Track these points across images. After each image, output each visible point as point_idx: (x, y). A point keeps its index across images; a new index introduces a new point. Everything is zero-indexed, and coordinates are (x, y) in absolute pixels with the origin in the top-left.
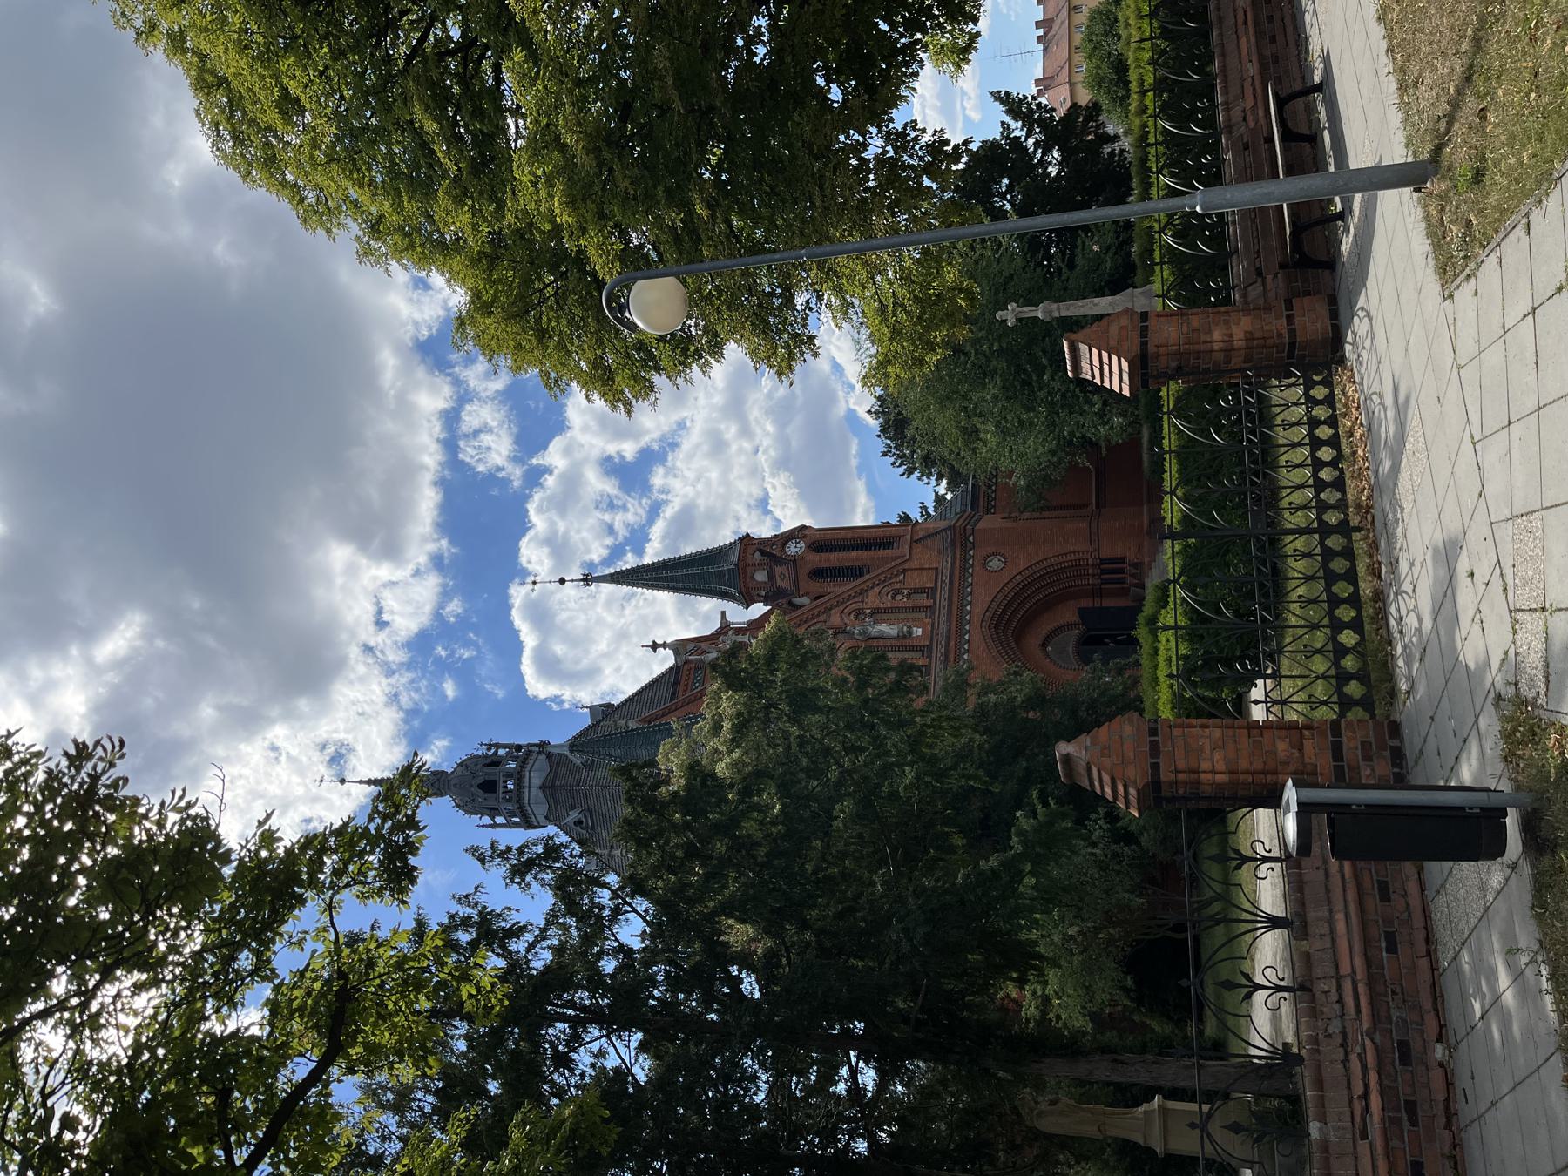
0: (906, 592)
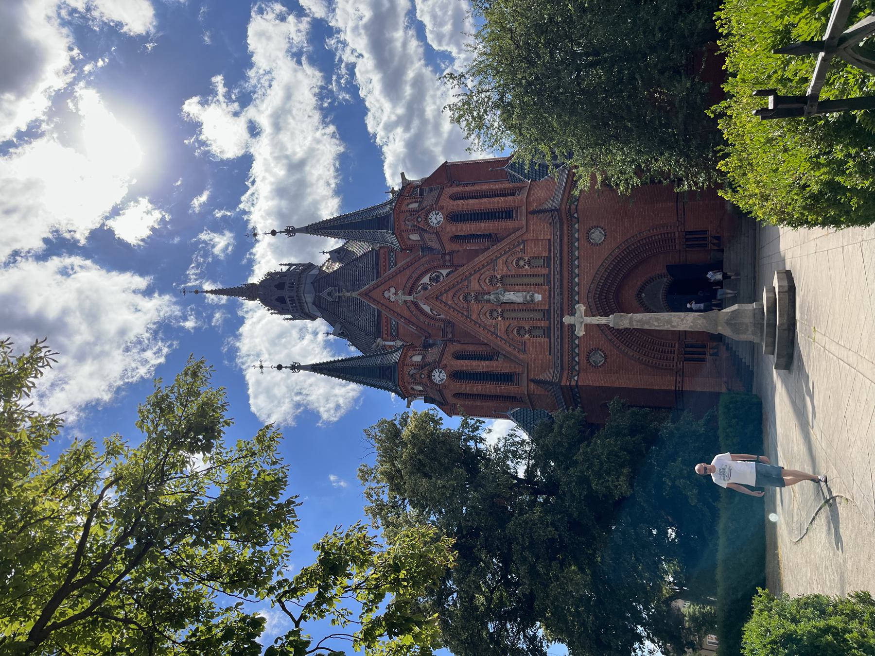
0: (526, 259)
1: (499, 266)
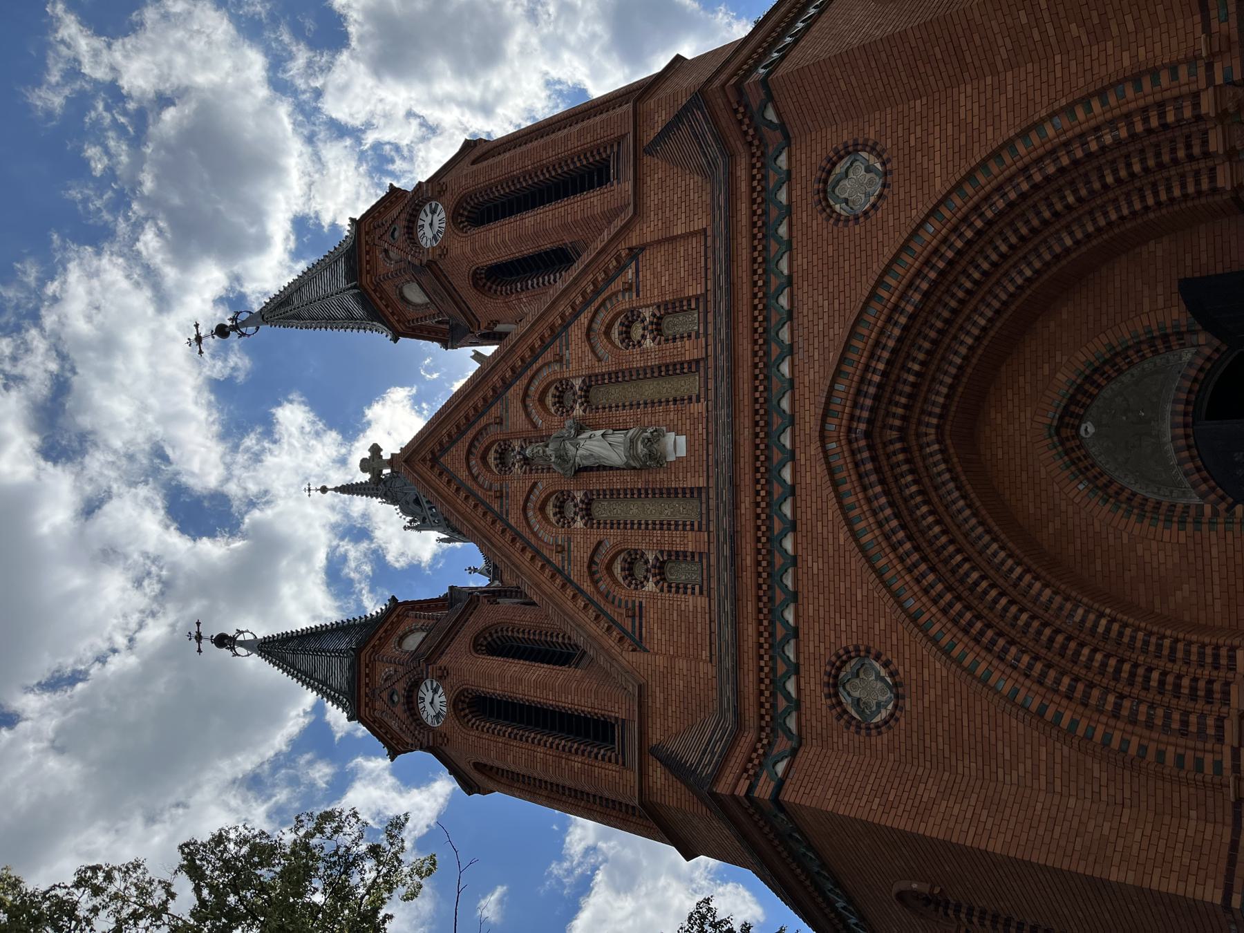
0: (647, 313)
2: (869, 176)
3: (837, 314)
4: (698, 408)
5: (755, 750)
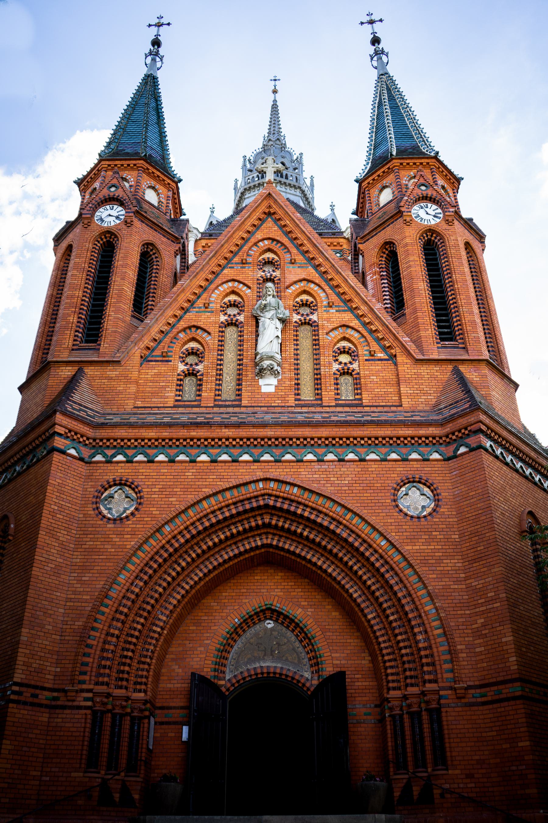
0: (355, 366)
1: (338, 315)
2: (420, 507)
3: (339, 488)
4: (291, 401)
5: (82, 436)
